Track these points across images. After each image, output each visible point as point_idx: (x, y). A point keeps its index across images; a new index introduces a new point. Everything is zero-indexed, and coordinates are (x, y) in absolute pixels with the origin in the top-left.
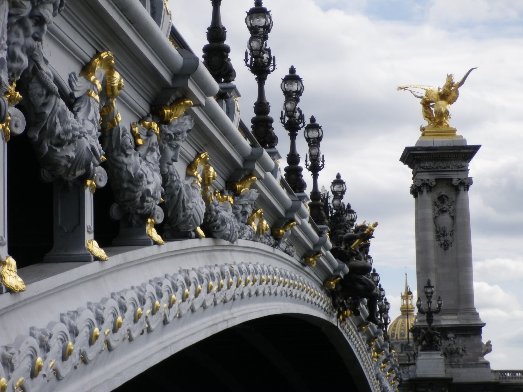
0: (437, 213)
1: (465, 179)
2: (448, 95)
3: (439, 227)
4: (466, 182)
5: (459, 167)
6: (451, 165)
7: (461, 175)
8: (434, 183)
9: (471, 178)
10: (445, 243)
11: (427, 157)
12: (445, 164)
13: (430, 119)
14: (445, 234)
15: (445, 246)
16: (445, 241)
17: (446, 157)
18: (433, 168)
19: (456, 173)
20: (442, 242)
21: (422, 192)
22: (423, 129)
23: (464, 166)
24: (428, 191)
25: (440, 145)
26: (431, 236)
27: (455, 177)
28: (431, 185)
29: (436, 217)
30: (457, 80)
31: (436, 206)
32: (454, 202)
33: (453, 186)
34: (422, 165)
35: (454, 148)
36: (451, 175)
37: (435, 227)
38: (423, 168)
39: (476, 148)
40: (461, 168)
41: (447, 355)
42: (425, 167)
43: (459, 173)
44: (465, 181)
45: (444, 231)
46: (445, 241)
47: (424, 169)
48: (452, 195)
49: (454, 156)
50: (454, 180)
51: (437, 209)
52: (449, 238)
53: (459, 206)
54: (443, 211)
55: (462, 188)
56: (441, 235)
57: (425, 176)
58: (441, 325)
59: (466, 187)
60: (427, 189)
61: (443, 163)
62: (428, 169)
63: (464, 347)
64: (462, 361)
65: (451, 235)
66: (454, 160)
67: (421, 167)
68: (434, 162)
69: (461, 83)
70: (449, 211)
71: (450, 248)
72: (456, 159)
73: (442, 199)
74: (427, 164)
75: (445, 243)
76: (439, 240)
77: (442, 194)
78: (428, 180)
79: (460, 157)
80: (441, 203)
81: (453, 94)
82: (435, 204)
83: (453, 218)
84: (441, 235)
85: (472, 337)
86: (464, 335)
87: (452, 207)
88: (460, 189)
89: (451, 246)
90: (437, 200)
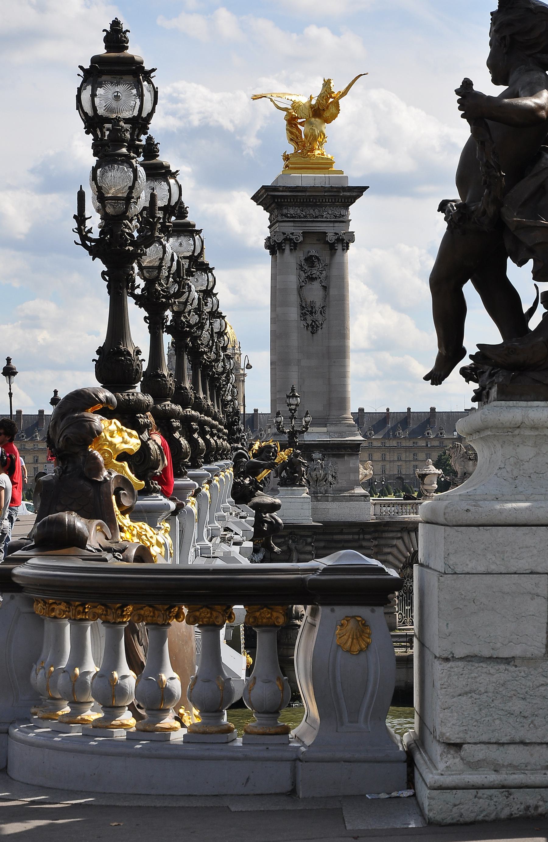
0: (303, 281)
1: (344, 234)
3: (306, 302)
5: (336, 217)
6: (325, 213)
7: (339, 228)
8: (301, 239)
9: (354, 232)
10: (313, 324)
11: (292, 201)
12: (316, 210)
13: (297, 143)
14: (314, 311)
15: (313, 328)
16: (313, 321)
17: (319, 202)
18: (300, 217)
19: (332, 225)
20: (310, 322)
21: (283, 251)
23: (343, 216)
24: (291, 250)
26: (294, 313)
27: (330, 230)
28: (296, 241)
29: (301, 287)
31: (302, 271)
32: (328, 266)
34: (285, 211)
35: (331, 189)
36: (326, 228)
37: (299, 300)
40: (339, 217)
41: (311, 484)
42: (289, 215)
43: (336, 224)
44: (344, 237)
45: (312, 307)
46: (313, 321)
47: (288, 217)
48: (324, 255)
49: (330, 201)
50: (329, 235)
52: (318, 316)
53: (334, 272)
54: (311, 279)
55: (339, 247)
56: (308, 313)
57: (288, 228)
58: (304, 441)
59: (345, 245)
60: (291, 246)
61: (314, 210)
62: (293, 217)
63: (335, 473)
64: (332, 492)
65: (321, 313)
66: (330, 206)
67: (282, 215)
68: (301, 208)
69: (345, 93)
70: (319, 278)
71: (320, 331)
72: (333, 205)
73: (310, 261)
74: (292, 211)
75: (313, 324)
76: (305, 319)
77: (310, 254)
78: (292, 234)
79: (338, 202)
80: (309, 267)
82: (301, 267)
83: (325, 288)
84: (308, 313)
86: (334, 456)
87: (324, 272)
88: (336, 248)
89: (321, 328)
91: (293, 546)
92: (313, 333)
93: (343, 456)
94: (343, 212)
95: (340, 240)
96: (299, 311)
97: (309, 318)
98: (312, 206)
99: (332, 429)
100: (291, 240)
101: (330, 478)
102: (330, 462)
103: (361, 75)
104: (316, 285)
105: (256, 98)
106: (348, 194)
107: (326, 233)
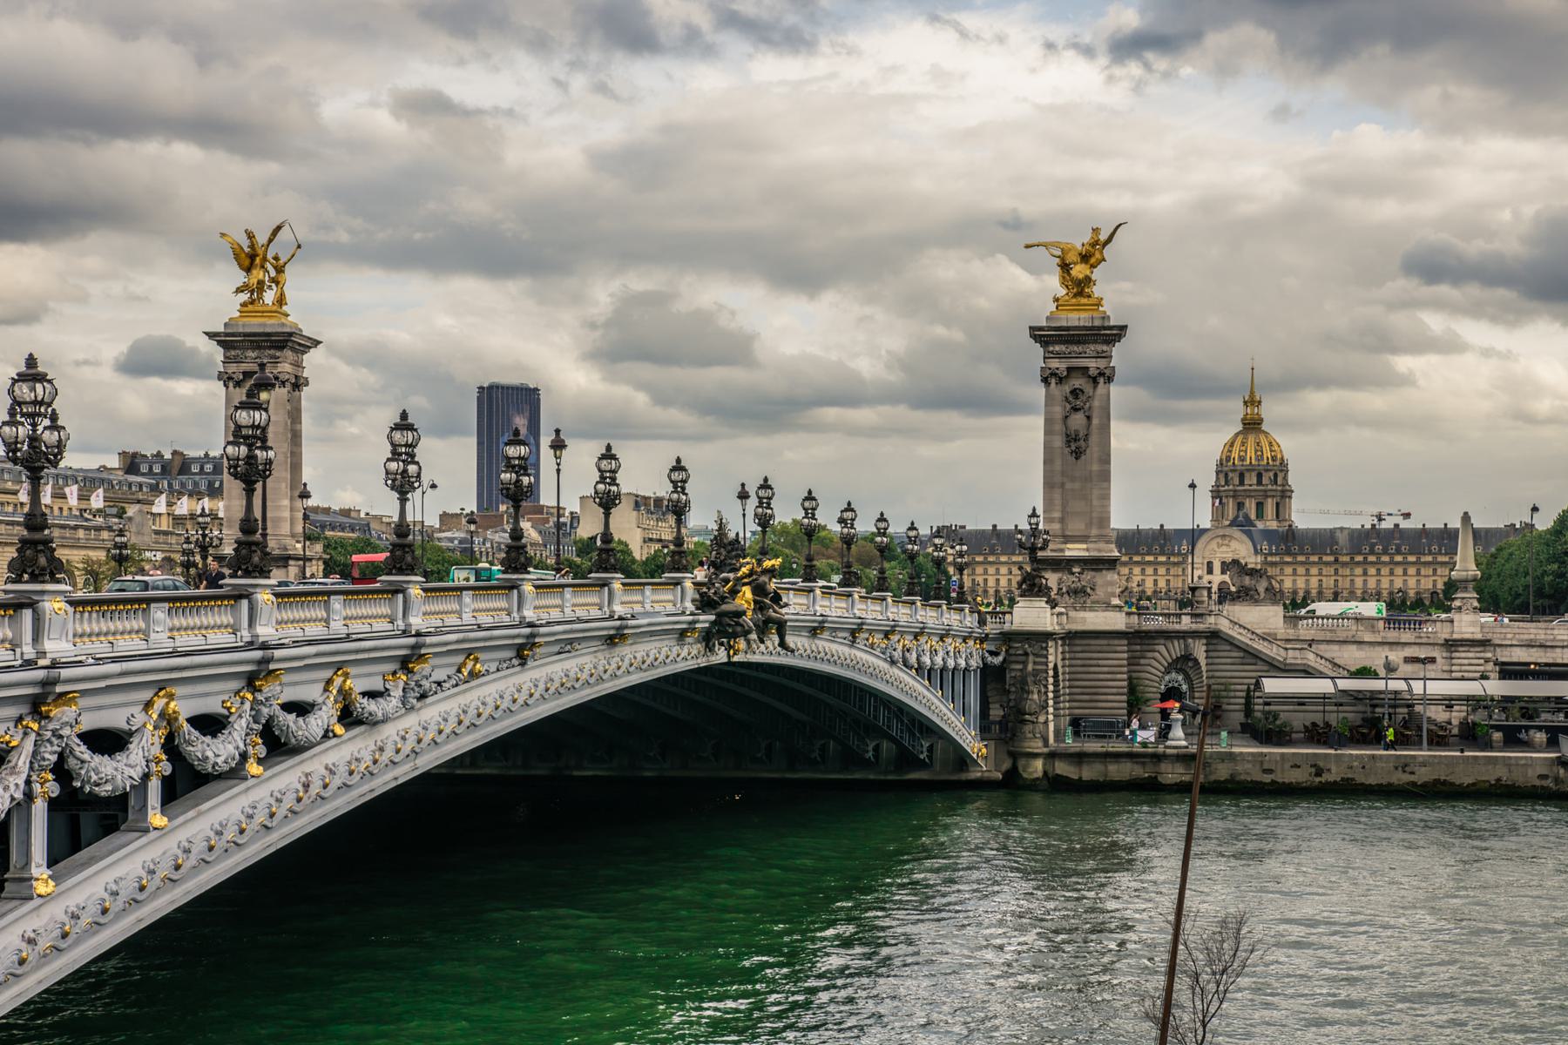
2: (1090, 256)
4: (1108, 372)
7: (1101, 363)
8: (1065, 373)
20: (1073, 448)
22: (1056, 300)
25: (1076, 324)
26: (1058, 442)
27: (1092, 364)
30: (1103, 237)
33: (1090, 376)
38: (1052, 352)
39: (1123, 328)
48: (1088, 388)
51: (1068, 406)
52: (1082, 443)
54: (1075, 409)
55: (1101, 380)
57: (1054, 364)
71: (1083, 457)
72: (1095, 342)
73: (1075, 393)
74: (1057, 348)
76: (1070, 446)
78: (1057, 369)
81: (1098, 255)
83: (1089, 418)
85: (1104, 572)
86: (1093, 570)
90: (1068, 395)
91: (1029, 650)
92: (1077, 459)
93: (1101, 570)
94: (1105, 348)
95: (1101, 374)
96: (1065, 439)
97: (1072, 444)
98: (1075, 343)
99: (1091, 546)
100: (1055, 375)
101: (1089, 590)
102: (1088, 576)
103: (1120, 225)
105: (1027, 247)
106: (1108, 332)
107: (1088, 368)
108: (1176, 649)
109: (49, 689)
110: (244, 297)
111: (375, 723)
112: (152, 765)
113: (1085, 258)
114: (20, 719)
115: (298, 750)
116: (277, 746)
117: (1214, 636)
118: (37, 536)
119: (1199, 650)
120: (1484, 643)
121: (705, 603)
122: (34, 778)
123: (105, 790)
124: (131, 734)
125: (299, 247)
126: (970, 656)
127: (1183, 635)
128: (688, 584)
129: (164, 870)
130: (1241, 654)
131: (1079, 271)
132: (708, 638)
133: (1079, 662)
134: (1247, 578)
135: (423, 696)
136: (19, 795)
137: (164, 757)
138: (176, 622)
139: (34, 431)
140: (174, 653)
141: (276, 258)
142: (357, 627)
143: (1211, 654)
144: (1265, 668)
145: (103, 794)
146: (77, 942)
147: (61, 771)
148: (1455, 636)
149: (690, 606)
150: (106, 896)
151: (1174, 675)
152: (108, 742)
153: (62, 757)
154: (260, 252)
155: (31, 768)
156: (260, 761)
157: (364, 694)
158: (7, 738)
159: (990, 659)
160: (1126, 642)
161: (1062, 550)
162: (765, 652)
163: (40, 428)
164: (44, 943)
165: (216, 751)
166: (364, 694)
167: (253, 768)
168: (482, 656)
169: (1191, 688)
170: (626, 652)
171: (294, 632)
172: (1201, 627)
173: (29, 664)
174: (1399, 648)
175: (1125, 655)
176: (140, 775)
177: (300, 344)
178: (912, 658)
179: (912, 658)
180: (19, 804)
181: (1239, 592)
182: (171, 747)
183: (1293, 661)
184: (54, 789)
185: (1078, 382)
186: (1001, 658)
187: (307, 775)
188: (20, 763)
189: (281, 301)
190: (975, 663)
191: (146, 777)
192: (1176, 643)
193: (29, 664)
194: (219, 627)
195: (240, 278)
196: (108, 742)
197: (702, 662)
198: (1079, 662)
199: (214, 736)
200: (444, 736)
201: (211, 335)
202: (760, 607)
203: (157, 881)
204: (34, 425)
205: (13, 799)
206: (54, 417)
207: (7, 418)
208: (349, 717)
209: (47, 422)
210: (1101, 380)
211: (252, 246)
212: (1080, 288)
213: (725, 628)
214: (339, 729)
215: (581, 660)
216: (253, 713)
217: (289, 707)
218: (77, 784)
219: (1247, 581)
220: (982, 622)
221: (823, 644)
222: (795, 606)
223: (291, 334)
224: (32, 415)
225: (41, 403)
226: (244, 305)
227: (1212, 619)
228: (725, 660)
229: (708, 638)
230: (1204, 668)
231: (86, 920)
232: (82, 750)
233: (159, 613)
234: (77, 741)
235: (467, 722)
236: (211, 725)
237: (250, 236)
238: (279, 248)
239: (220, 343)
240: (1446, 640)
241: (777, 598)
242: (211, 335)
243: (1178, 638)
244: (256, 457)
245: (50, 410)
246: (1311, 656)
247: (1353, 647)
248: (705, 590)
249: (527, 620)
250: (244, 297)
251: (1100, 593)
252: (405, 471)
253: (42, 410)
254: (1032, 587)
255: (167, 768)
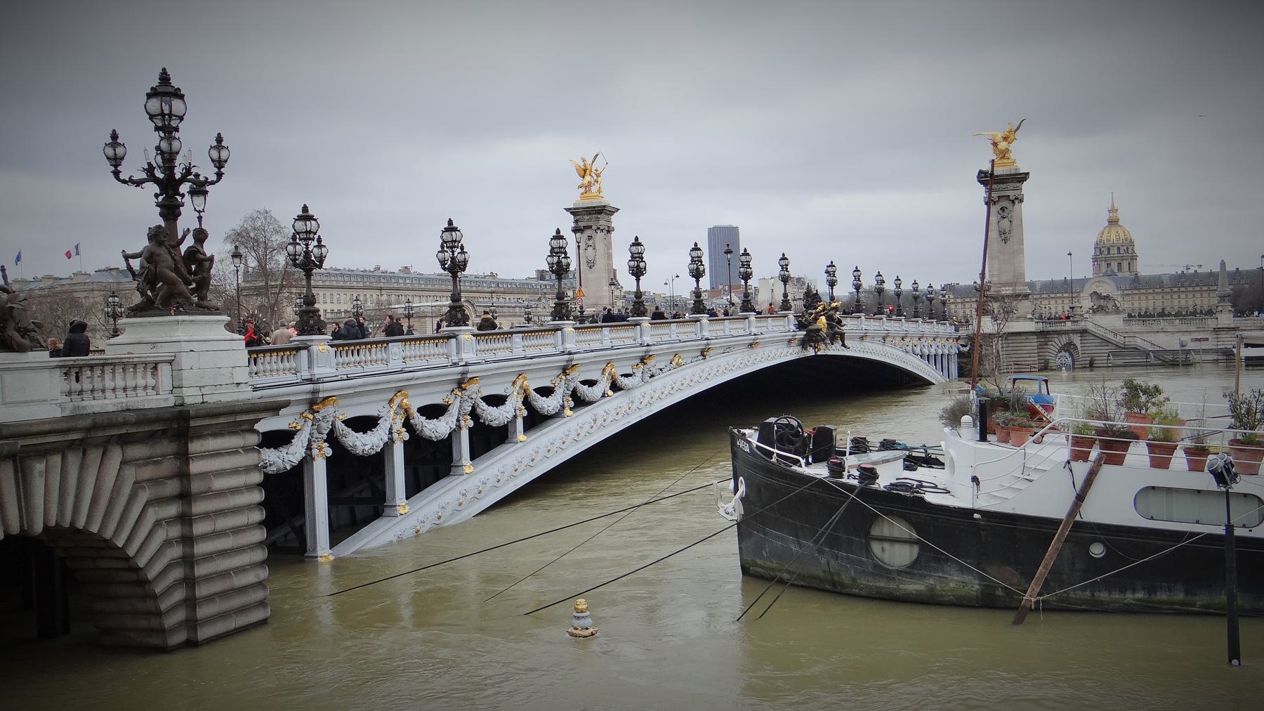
4: (1020, 197)
7: (1016, 192)
15: (1005, 241)
27: (1011, 194)
39: (1027, 174)
53: (1014, 214)
55: (1016, 201)
73: (1002, 209)
101: (1014, 311)
104: (1006, 220)
108: (1064, 339)
109: (464, 376)
110: (582, 190)
111: (629, 389)
112: (518, 412)
113: (1005, 139)
114: (453, 391)
115: (590, 403)
116: (580, 402)
117: (1084, 332)
118: (457, 304)
119: (1076, 340)
120: (1234, 329)
121: (800, 326)
122: (461, 418)
123: (495, 424)
124: (506, 397)
125: (607, 164)
126: (952, 348)
127: (1067, 332)
128: (791, 317)
129: (527, 461)
130: (1100, 341)
131: (1003, 145)
132: (804, 344)
133: (1011, 348)
134: (1102, 300)
135: (652, 376)
136: (454, 427)
137: (523, 407)
138: (526, 343)
139: (453, 254)
140: (525, 358)
141: (596, 170)
142: (616, 343)
143: (1083, 342)
144: (1114, 347)
145: (494, 425)
146: (486, 495)
147: (474, 414)
148: (1219, 326)
149: (793, 328)
150: (499, 473)
151: (1063, 353)
152: (496, 401)
153: (473, 407)
154: (588, 167)
155: (459, 414)
156: (571, 409)
157: (622, 376)
158: (447, 400)
159: (962, 349)
160: (1036, 337)
161: (1000, 291)
162: (835, 350)
163: (456, 254)
164: (470, 496)
165: (547, 405)
166: (622, 376)
167: (568, 412)
168: (682, 356)
169: (1073, 361)
170: (758, 351)
171: (586, 347)
172: (1077, 327)
173: (455, 365)
174: (1187, 333)
175: (1036, 344)
176: (512, 416)
177: (609, 211)
178: (918, 350)
179: (918, 350)
180: (455, 430)
181: (1097, 308)
182: (527, 402)
183: (1129, 343)
184: (471, 424)
185: (1004, 203)
186: (968, 348)
187: (595, 415)
188: (454, 411)
189: (599, 191)
190: (954, 351)
191: (515, 417)
192: (1063, 336)
193: (455, 365)
194: (547, 345)
195: (579, 181)
196: (496, 401)
197: (802, 355)
198: (1011, 348)
199: (547, 397)
200: (664, 395)
201: (568, 210)
202: (830, 326)
203: (523, 467)
204: (453, 252)
205: (451, 428)
206: (462, 248)
207: (440, 249)
208: (615, 387)
209: (459, 250)
210: (1016, 201)
211: (585, 165)
212: (1003, 154)
213: (812, 338)
214: (610, 393)
215: (735, 356)
216: (566, 385)
217: (584, 383)
218: (482, 421)
219: (1102, 302)
220: (957, 330)
221: (867, 344)
222: (849, 325)
223: (605, 206)
224: (452, 248)
225: (455, 241)
226: (582, 194)
227: (1083, 323)
228: (814, 354)
229: (804, 344)
230: (1080, 349)
231: (489, 485)
232: (483, 405)
233: (517, 338)
234: (481, 400)
235: (676, 388)
236: (546, 392)
237: (584, 161)
238: (598, 165)
239: (571, 213)
240: (1214, 329)
241: (839, 322)
242: (568, 210)
243: (1066, 334)
244: (561, 262)
245: (460, 245)
246: (1139, 340)
247: (1163, 334)
248: (800, 319)
249: (705, 337)
250: (582, 190)
251: (1020, 312)
252: (638, 266)
253: (456, 244)
254: (982, 311)
255: (525, 413)
